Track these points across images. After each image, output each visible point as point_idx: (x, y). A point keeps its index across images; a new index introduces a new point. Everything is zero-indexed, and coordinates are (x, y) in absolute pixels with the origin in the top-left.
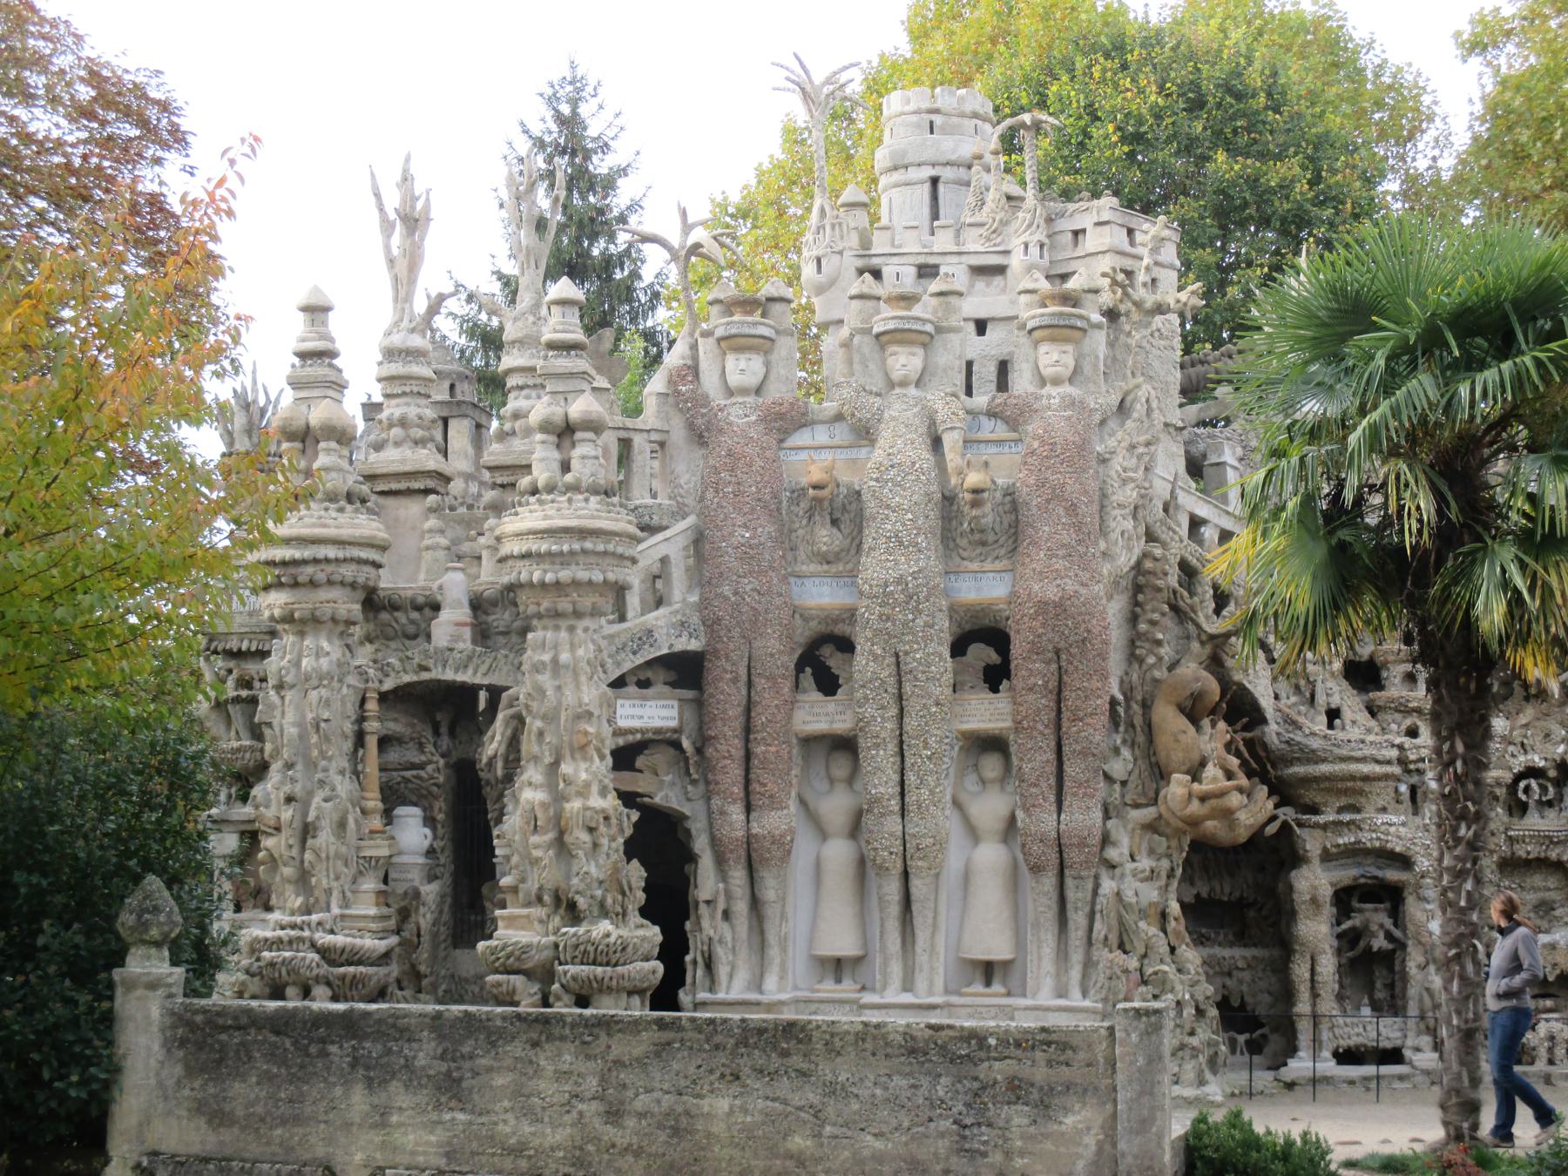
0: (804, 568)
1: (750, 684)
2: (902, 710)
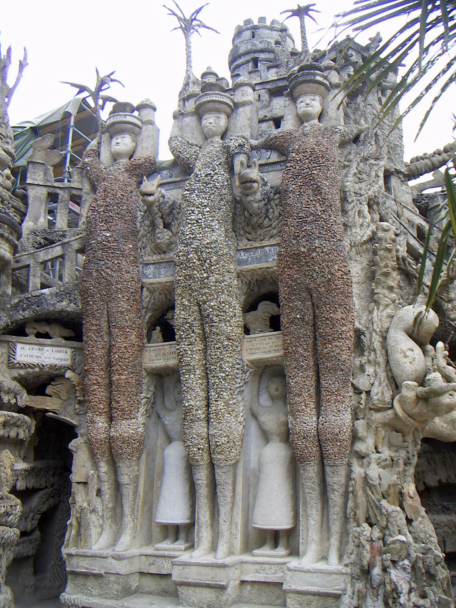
0: (150, 258)
1: (110, 334)
2: (206, 346)
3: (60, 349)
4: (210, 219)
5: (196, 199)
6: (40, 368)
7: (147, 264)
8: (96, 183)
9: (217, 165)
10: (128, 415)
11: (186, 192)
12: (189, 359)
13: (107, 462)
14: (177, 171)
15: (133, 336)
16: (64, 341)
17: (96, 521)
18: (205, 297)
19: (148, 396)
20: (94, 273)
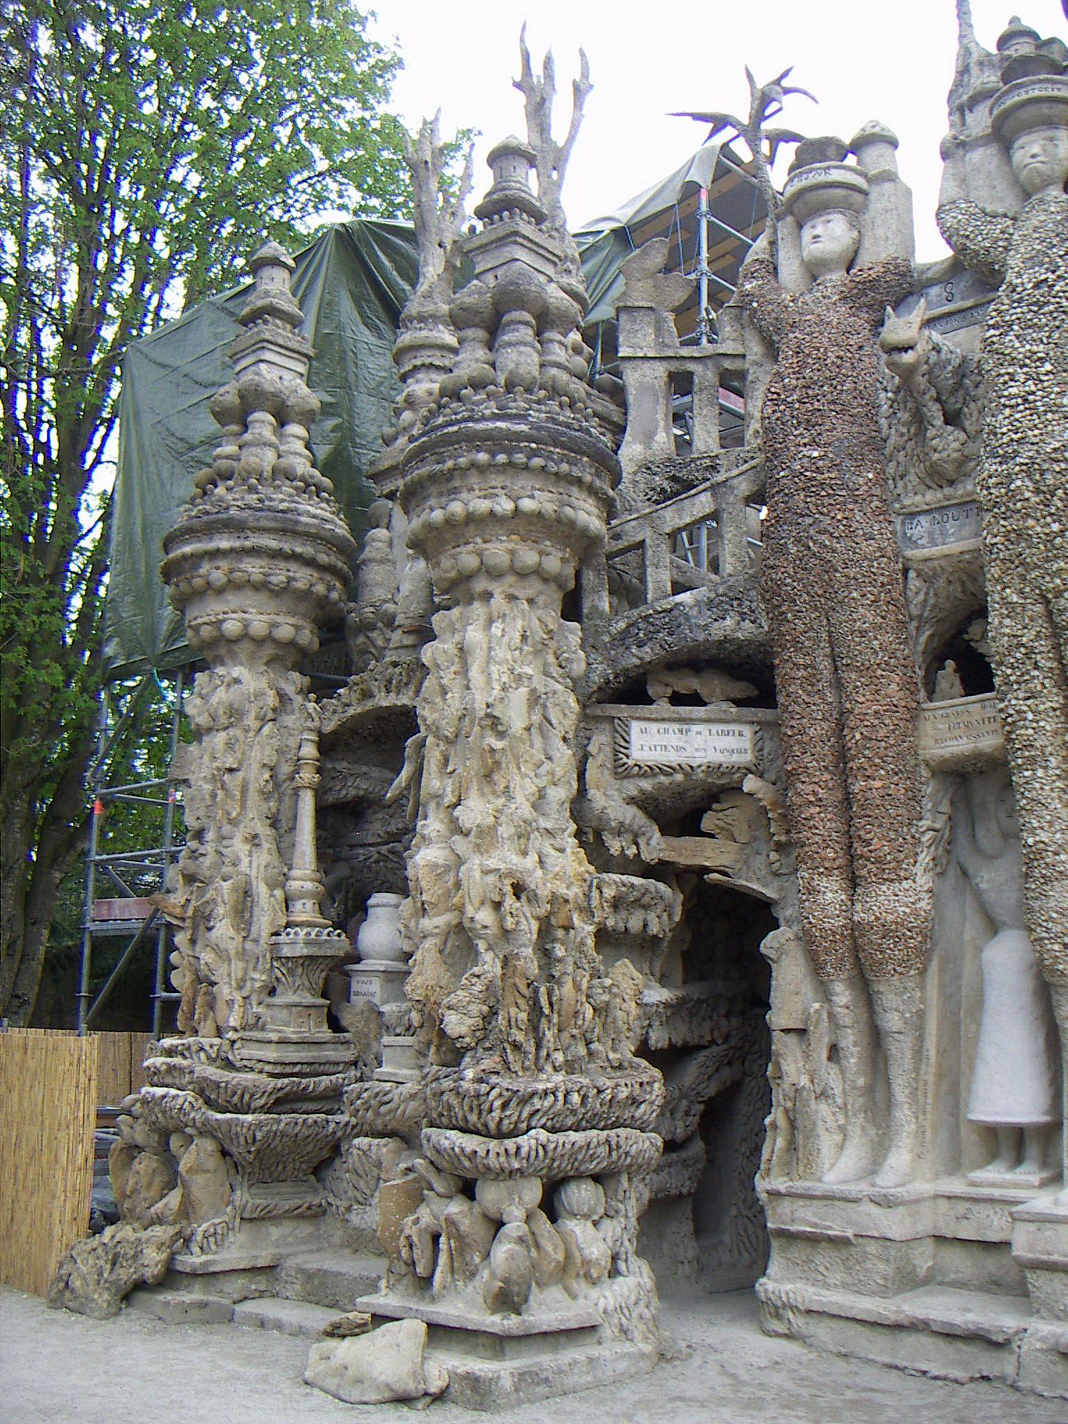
0: (918, 498)
1: (838, 685)
3: (725, 727)
4: (1056, 389)
5: (1017, 345)
6: (686, 774)
7: (912, 515)
8: (776, 338)
9: (1061, 257)
10: (894, 873)
11: (992, 332)
12: (1031, 731)
13: (850, 982)
14: (962, 284)
15: (894, 686)
16: (734, 710)
17: (830, 1119)
18: (1058, 581)
19: (937, 826)
20: (790, 546)
